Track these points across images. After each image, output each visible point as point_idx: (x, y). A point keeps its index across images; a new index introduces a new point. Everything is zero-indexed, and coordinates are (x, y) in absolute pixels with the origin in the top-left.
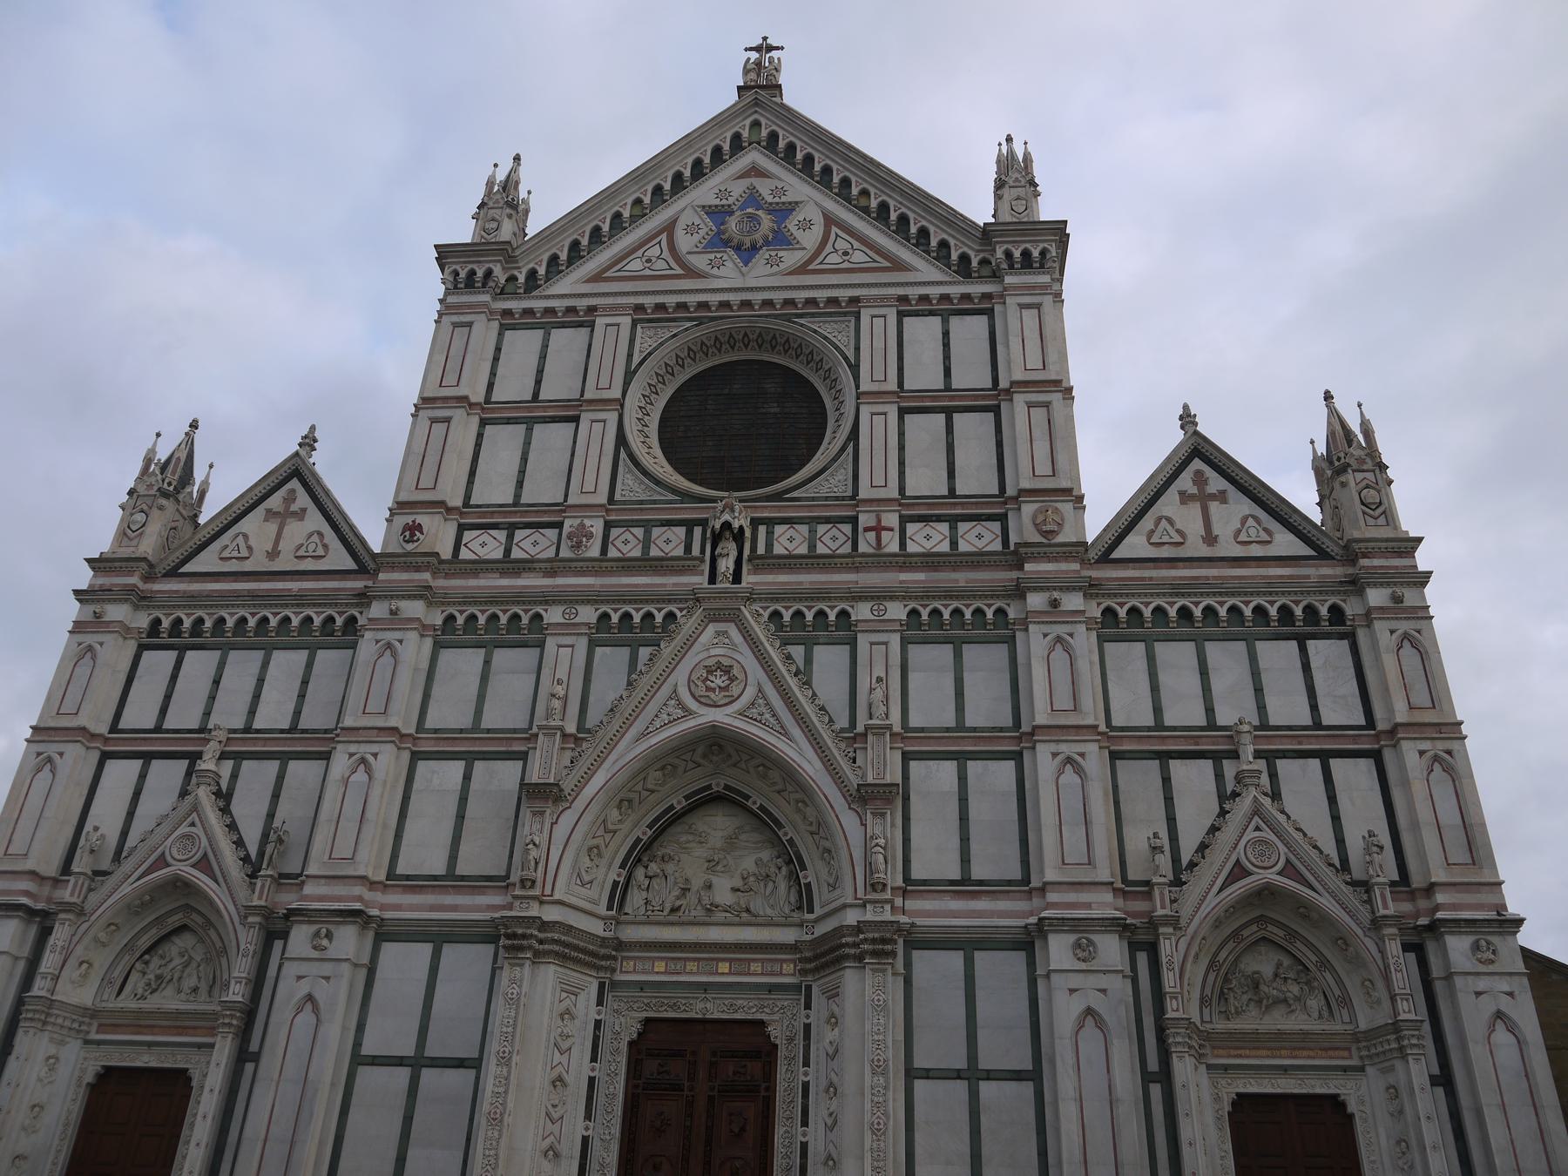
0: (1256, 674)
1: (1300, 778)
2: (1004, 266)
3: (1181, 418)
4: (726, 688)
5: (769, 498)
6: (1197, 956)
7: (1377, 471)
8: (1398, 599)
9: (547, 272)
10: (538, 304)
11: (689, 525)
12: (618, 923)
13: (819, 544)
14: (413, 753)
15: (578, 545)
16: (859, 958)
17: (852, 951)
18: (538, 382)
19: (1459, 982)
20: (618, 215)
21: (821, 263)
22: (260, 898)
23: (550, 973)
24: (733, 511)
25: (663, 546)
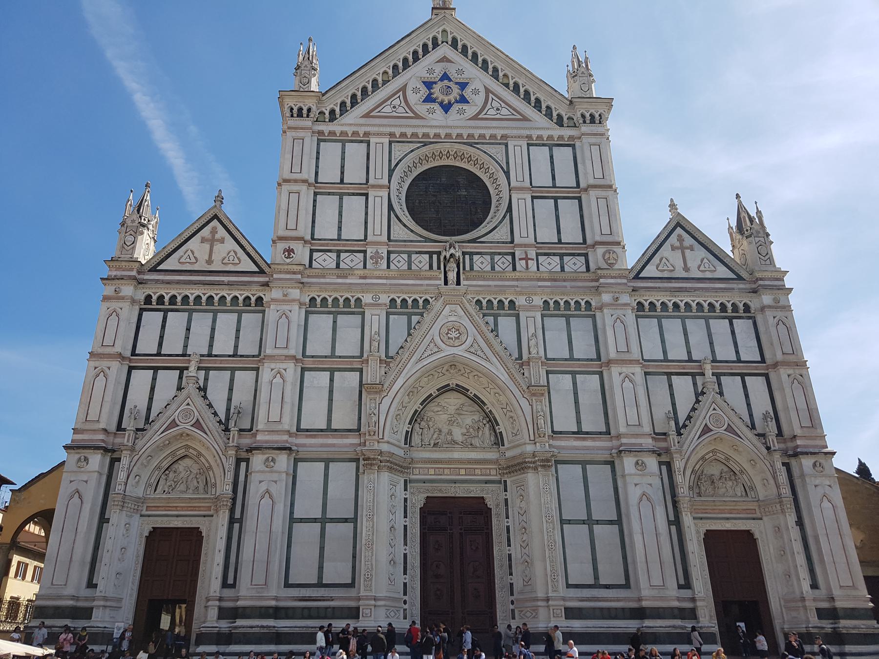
0: (710, 335)
2: (581, 121)
3: (670, 206)
4: (458, 338)
5: (469, 241)
7: (765, 237)
8: (777, 301)
11: (431, 254)
14: (302, 368)
15: (377, 263)
16: (536, 469)
18: (342, 173)
21: (485, 114)
22: (233, 442)
23: (385, 476)
24: (455, 248)
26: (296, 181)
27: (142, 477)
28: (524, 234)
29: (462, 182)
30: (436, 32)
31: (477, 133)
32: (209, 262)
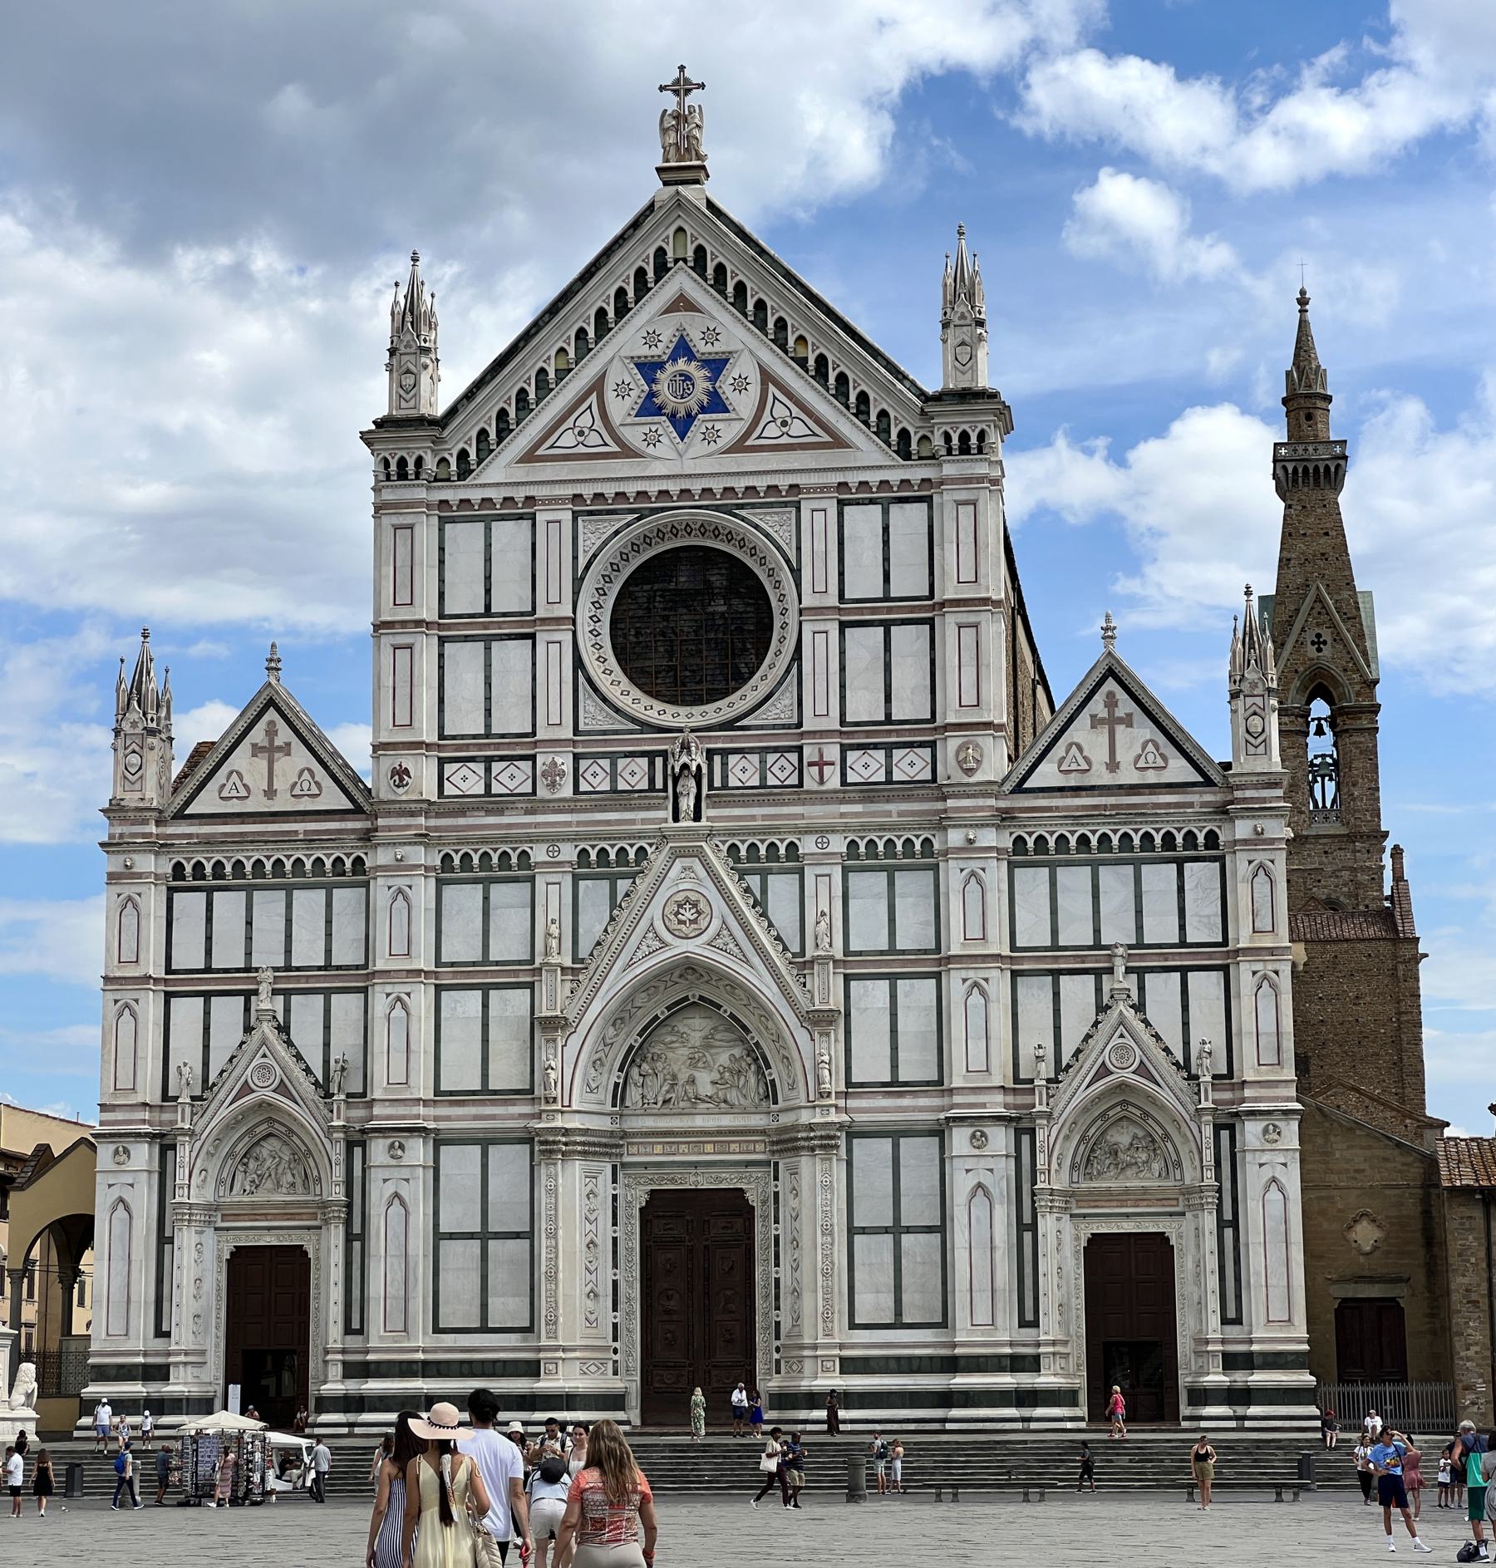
1: (1162, 990)
2: (943, 452)
4: (694, 922)
6: (1067, 1138)
9: (478, 450)
10: (476, 495)
11: (651, 755)
12: (621, 1115)
13: (769, 775)
14: (436, 985)
15: (553, 785)
16: (812, 1149)
17: (806, 1144)
18: (488, 591)
19: (1249, 1157)
20: (542, 371)
23: (577, 1166)
24: (689, 753)
25: (628, 778)
26: (404, 624)
27: (210, 1171)
28: (821, 710)
29: (718, 584)
30: (662, 237)
31: (740, 484)
32: (270, 793)
